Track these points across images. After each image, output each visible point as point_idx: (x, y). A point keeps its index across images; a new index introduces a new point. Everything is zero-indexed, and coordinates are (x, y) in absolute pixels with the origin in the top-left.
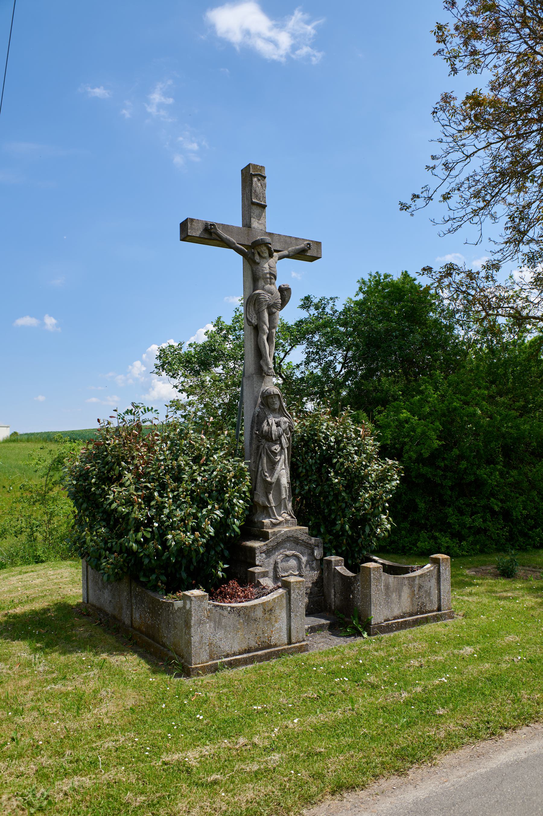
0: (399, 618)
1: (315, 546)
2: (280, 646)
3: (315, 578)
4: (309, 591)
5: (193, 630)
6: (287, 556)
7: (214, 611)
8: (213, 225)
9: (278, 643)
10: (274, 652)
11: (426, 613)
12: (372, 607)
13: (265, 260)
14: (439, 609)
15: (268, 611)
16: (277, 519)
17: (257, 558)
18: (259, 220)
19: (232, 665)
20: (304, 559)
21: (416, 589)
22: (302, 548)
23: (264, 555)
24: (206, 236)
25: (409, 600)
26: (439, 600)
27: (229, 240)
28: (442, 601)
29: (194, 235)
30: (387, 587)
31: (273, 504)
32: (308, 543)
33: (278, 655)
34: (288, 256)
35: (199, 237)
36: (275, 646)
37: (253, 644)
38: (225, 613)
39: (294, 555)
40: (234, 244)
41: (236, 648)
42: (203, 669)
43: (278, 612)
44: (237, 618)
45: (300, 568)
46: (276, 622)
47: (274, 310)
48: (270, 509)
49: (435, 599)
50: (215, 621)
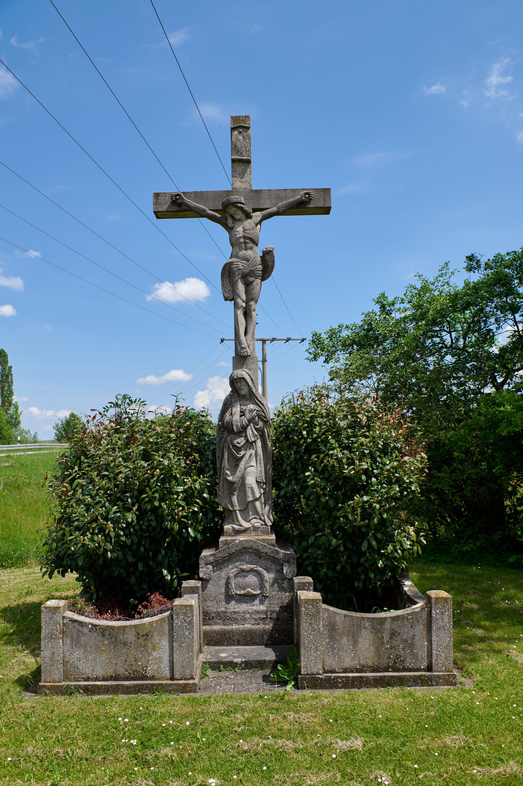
0: (352, 672)
1: (285, 562)
2: (159, 679)
3: (286, 601)
4: (274, 616)
5: (42, 644)
6: (243, 571)
7: (70, 627)
8: (178, 195)
9: (157, 676)
10: (147, 685)
11: (405, 670)
12: (302, 652)
13: (240, 223)
14: (429, 668)
15: (143, 636)
16: (241, 526)
17: (201, 570)
18: (242, 178)
19: (89, 691)
20: (269, 577)
21: (386, 636)
22: (268, 563)
23: (210, 567)
24: (175, 208)
25: (372, 649)
26: (430, 655)
27: (198, 208)
28: (434, 658)
29: (160, 210)
30: (332, 627)
31: (237, 508)
32: (273, 557)
33: (151, 689)
34: (277, 213)
35: (166, 211)
36: (153, 678)
37: (121, 671)
38: (86, 630)
39: (252, 570)
40: (205, 211)
41: (100, 673)
42: (50, 688)
43: (156, 639)
44: (100, 638)
45: (262, 586)
46: (154, 649)
47: (251, 279)
48: (234, 513)
49: (423, 654)
50: (72, 638)
